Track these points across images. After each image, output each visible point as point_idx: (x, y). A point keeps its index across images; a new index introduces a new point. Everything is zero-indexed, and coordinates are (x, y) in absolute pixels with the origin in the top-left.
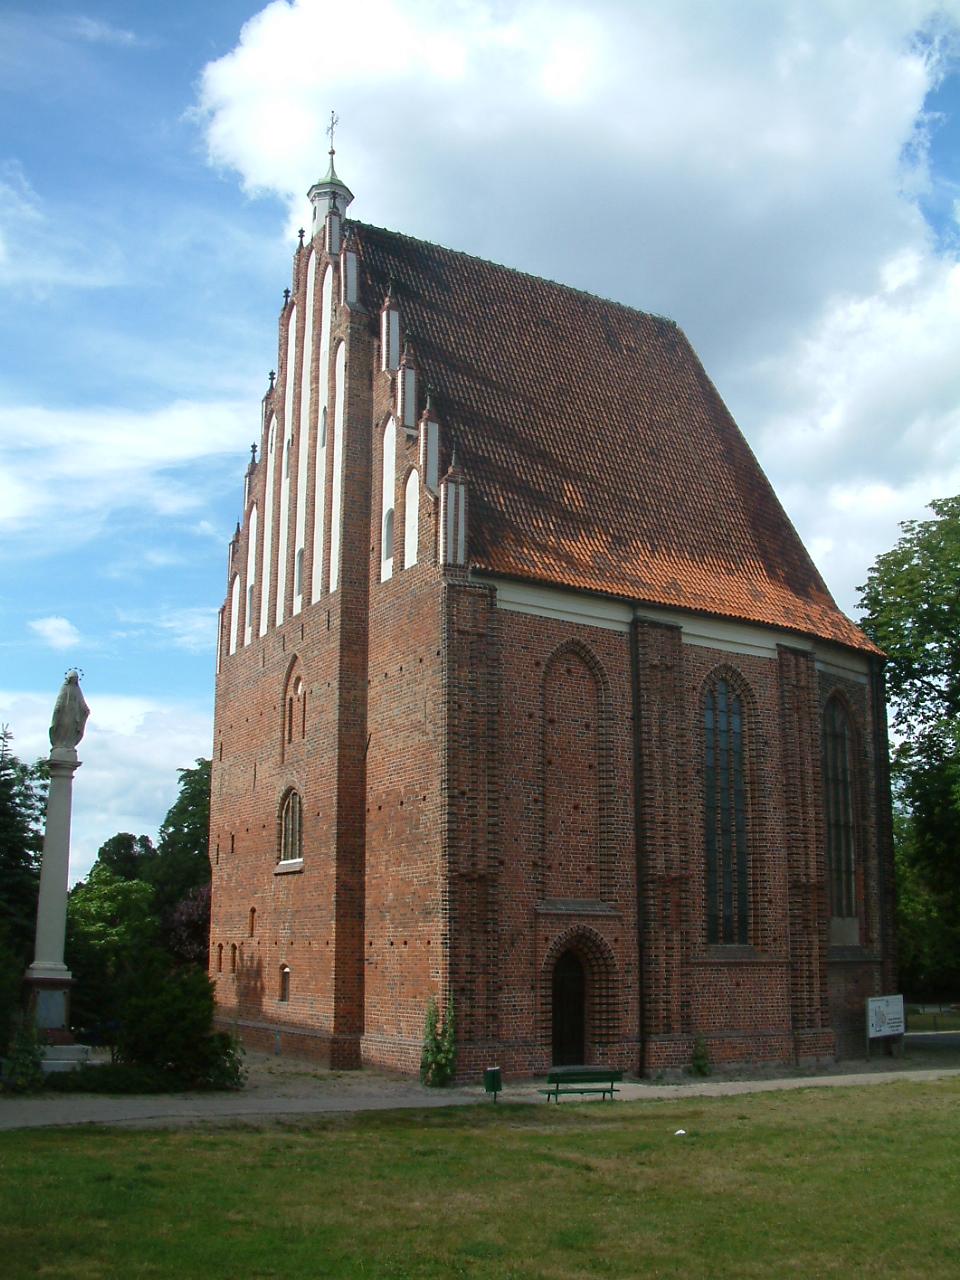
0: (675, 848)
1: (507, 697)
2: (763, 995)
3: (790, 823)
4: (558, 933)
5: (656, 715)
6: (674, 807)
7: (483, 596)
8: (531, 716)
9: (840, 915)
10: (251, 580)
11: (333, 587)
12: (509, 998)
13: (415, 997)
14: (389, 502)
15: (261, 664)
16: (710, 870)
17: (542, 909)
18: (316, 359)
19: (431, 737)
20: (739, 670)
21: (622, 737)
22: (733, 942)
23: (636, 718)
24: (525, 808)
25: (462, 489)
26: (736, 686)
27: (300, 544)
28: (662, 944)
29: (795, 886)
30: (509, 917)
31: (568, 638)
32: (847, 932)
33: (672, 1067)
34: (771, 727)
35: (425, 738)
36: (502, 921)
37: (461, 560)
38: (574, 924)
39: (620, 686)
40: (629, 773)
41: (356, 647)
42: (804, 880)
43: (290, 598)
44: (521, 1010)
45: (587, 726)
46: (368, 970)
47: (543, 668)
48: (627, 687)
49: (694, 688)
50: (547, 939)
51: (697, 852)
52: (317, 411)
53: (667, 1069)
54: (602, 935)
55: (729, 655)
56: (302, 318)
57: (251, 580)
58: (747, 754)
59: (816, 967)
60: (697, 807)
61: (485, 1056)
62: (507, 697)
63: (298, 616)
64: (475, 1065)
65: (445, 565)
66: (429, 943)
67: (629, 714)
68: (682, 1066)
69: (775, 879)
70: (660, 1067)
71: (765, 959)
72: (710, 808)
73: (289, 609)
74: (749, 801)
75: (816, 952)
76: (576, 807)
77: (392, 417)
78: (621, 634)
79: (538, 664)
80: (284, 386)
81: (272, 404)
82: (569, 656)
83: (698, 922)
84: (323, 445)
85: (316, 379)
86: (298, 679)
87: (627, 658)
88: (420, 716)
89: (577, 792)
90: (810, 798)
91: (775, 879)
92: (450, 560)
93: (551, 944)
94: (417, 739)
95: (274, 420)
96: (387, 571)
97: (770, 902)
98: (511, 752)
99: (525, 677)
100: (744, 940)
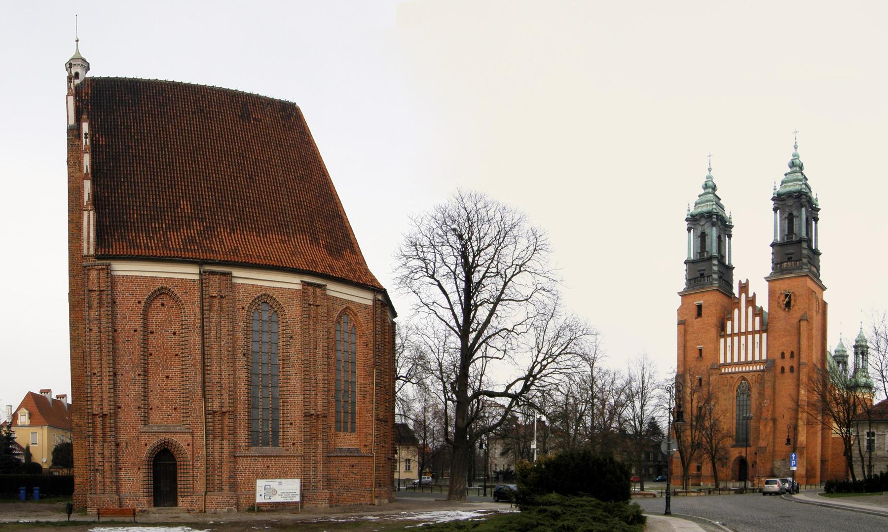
0: (225, 396)
3: (306, 380)
5: (214, 324)
6: (225, 375)
9: (346, 430)
16: (252, 406)
17: (145, 429)
21: (195, 338)
22: (268, 445)
23: (203, 326)
28: (217, 446)
29: (307, 415)
31: (159, 286)
32: (347, 441)
34: (297, 329)
38: (163, 437)
39: (193, 310)
40: (198, 357)
42: (313, 412)
48: (198, 310)
49: (243, 308)
51: (242, 398)
58: (281, 344)
59: (320, 458)
60: (242, 374)
67: (199, 325)
69: (295, 411)
71: (288, 453)
72: (250, 373)
74: (281, 370)
75: (320, 450)
76: (167, 377)
79: (139, 302)
82: (162, 296)
83: (242, 434)
87: (198, 294)
90: (320, 368)
91: (295, 411)
93: (148, 447)
97: (291, 424)
100: (276, 444)
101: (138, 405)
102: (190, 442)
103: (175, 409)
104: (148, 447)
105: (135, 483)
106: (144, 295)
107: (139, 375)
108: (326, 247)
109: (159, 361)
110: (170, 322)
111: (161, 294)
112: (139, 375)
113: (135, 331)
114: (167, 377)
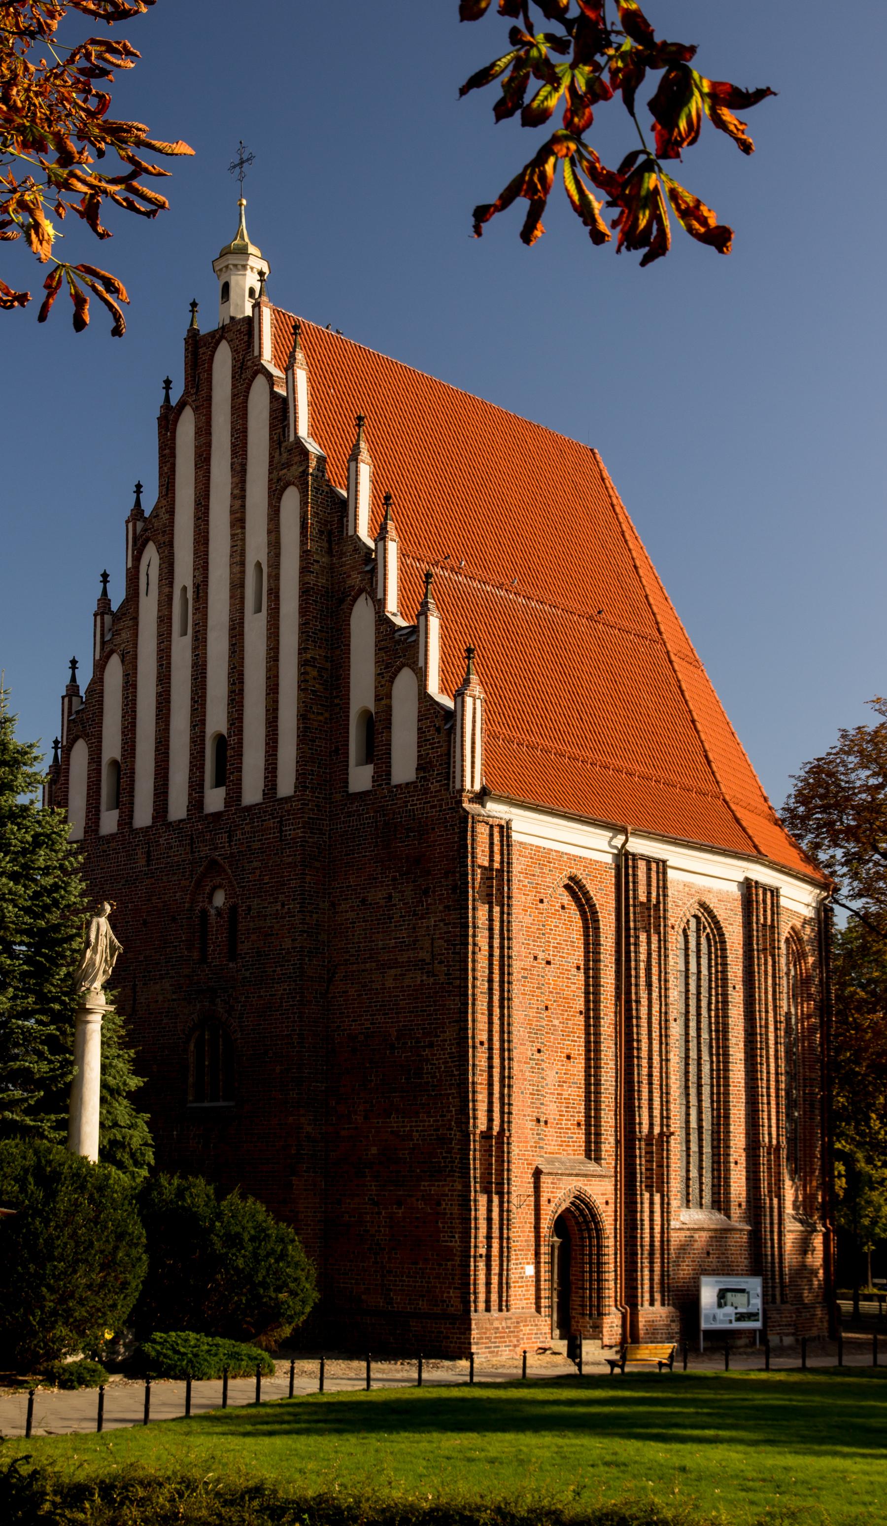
8: (535, 958)
10: (112, 748)
11: (286, 786)
14: (361, 694)
15: (143, 862)
18: (239, 494)
19: (442, 978)
27: (217, 721)
35: (432, 980)
41: (317, 864)
43: (196, 787)
50: (549, 1201)
52: (242, 564)
56: (204, 432)
57: (112, 748)
63: (217, 815)
66: (439, 1204)
73: (196, 802)
77: (363, 596)
79: (541, 901)
80: (171, 512)
81: (149, 530)
84: (258, 610)
85: (238, 521)
86: (214, 889)
88: (423, 955)
94: (419, 979)
95: (151, 553)
96: (361, 778)
109: (556, 1022)
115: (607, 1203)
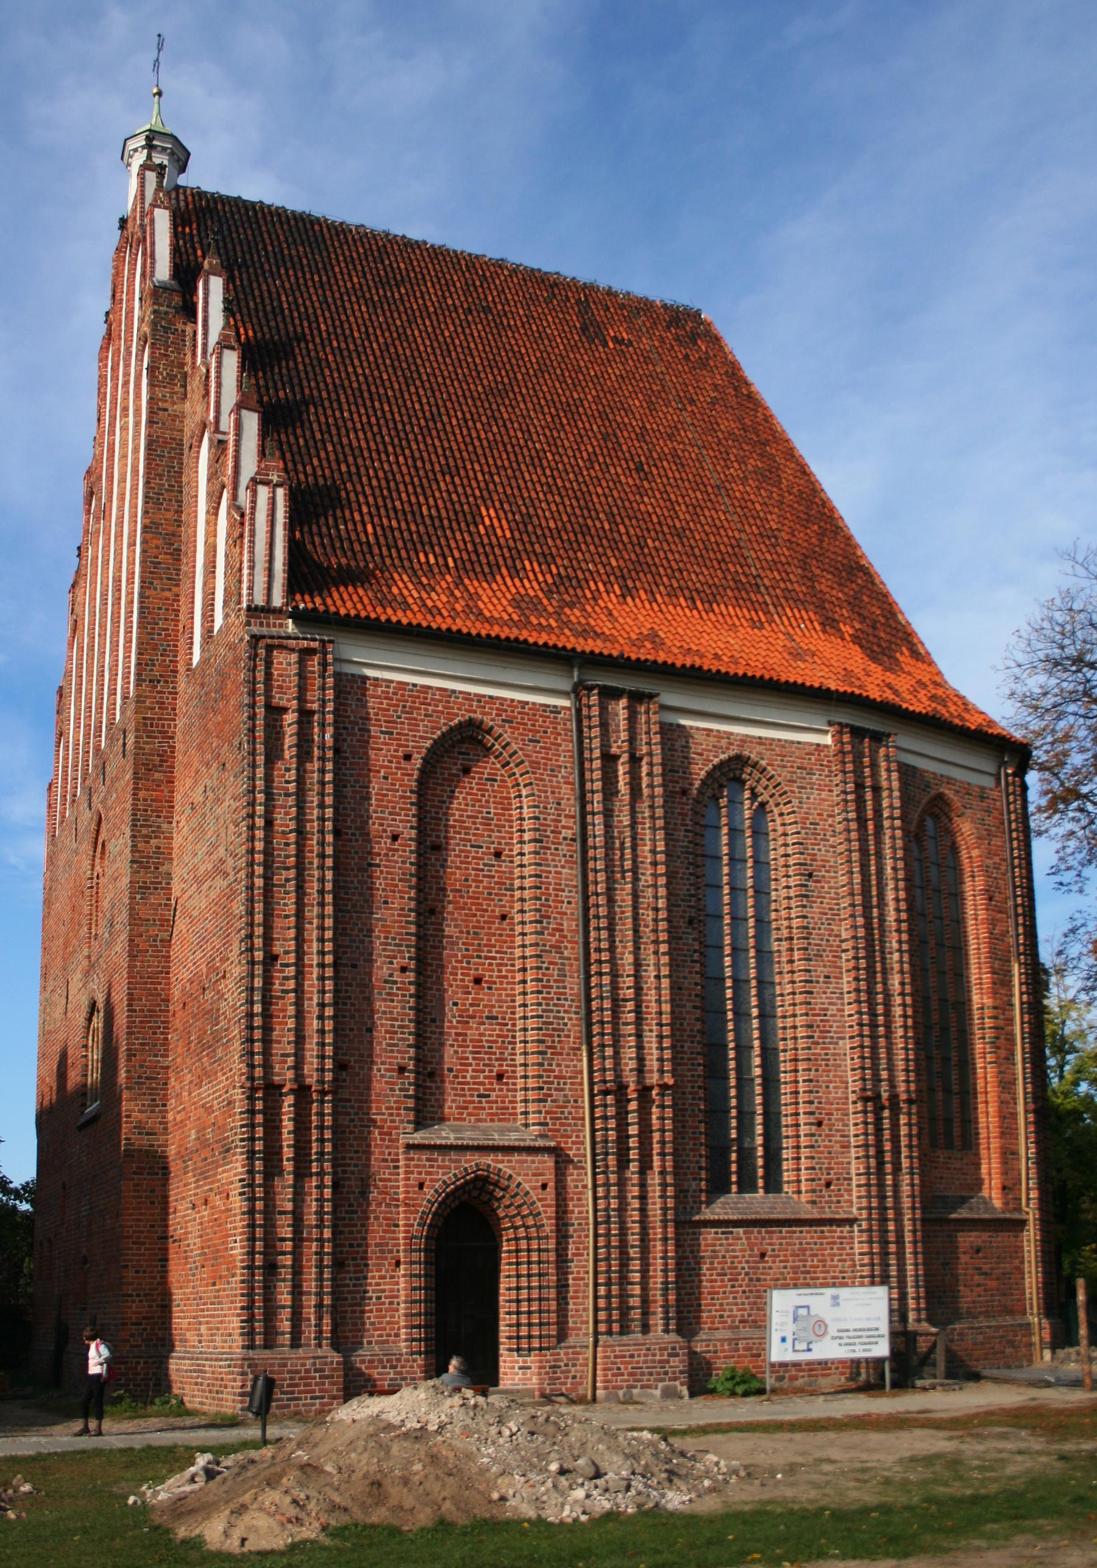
1: (354, 810)
2: (808, 1272)
4: (445, 1174)
7: (306, 654)
8: (395, 838)
12: (358, 1279)
13: (214, 1284)
17: (418, 1137)
20: (763, 763)
24: (386, 982)
25: (280, 492)
26: (760, 789)
30: (356, 1152)
33: (642, 1387)
36: (344, 1158)
37: (278, 601)
44: (379, 1298)
45: (498, 854)
46: (172, 1247)
47: (417, 762)
50: (421, 1186)
53: (635, 1391)
54: (520, 1179)
55: (745, 740)
61: (307, 1371)
62: (354, 810)
64: (289, 1386)
65: (249, 608)
68: (660, 1385)
70: (621, 1388)
76: (478, 981)
78: (556, 710)
79: (408, 757)
89: (479, 957)
92: (259, 600)
93: (428, 1193)
98: (360, 894)
99: (386, 778)
101: (398, 1060)
102: (550, 1177)
103: (500, 1077)
104: (428, 1193)
105: (395, 1293)
106: (422, 738)
107: (404, 969)
108: (856, 639)
110: (487, 822)
111: (462, 741)
112: (404, 969)
113: (395, 838)
114: (478, 981)
115: (544, 1186)
